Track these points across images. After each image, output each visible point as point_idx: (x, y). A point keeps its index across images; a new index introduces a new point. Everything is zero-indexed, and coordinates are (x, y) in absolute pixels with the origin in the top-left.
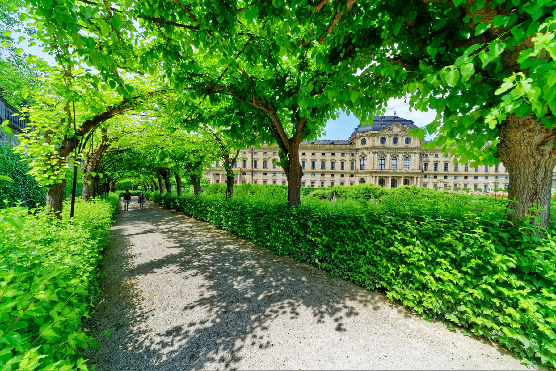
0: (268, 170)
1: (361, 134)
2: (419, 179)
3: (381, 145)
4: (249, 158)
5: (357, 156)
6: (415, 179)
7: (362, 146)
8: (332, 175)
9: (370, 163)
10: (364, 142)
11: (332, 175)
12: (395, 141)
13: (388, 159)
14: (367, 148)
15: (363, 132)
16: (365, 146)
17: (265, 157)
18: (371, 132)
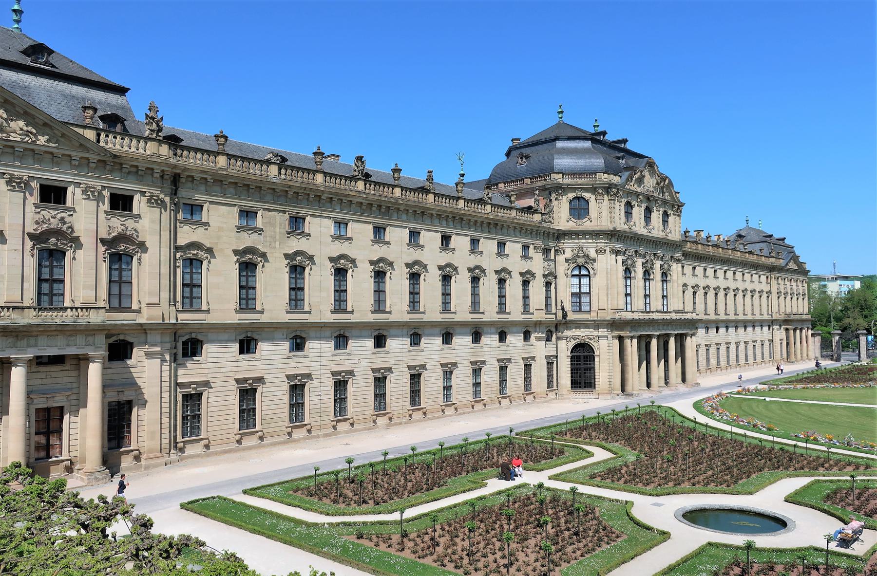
0: (265, 319)
1: (567, 181)
3: (626, 227)
4: (151, 242)
5: (561, 259)
7: (571, 225)
8: (502, 337)
10: (579, 209)
11: (502, 337)
14: (595, 234)
15: (573, 174)
16: (587, 225)
17: (247, 240)
18: (605, 178)
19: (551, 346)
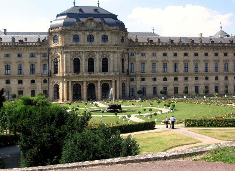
2: (118, 83)
5: (50, 56)
6: (113, 84)
9: (63, 65)
12: (91, 39)
13: (84, 60)
19: (46, 85)
